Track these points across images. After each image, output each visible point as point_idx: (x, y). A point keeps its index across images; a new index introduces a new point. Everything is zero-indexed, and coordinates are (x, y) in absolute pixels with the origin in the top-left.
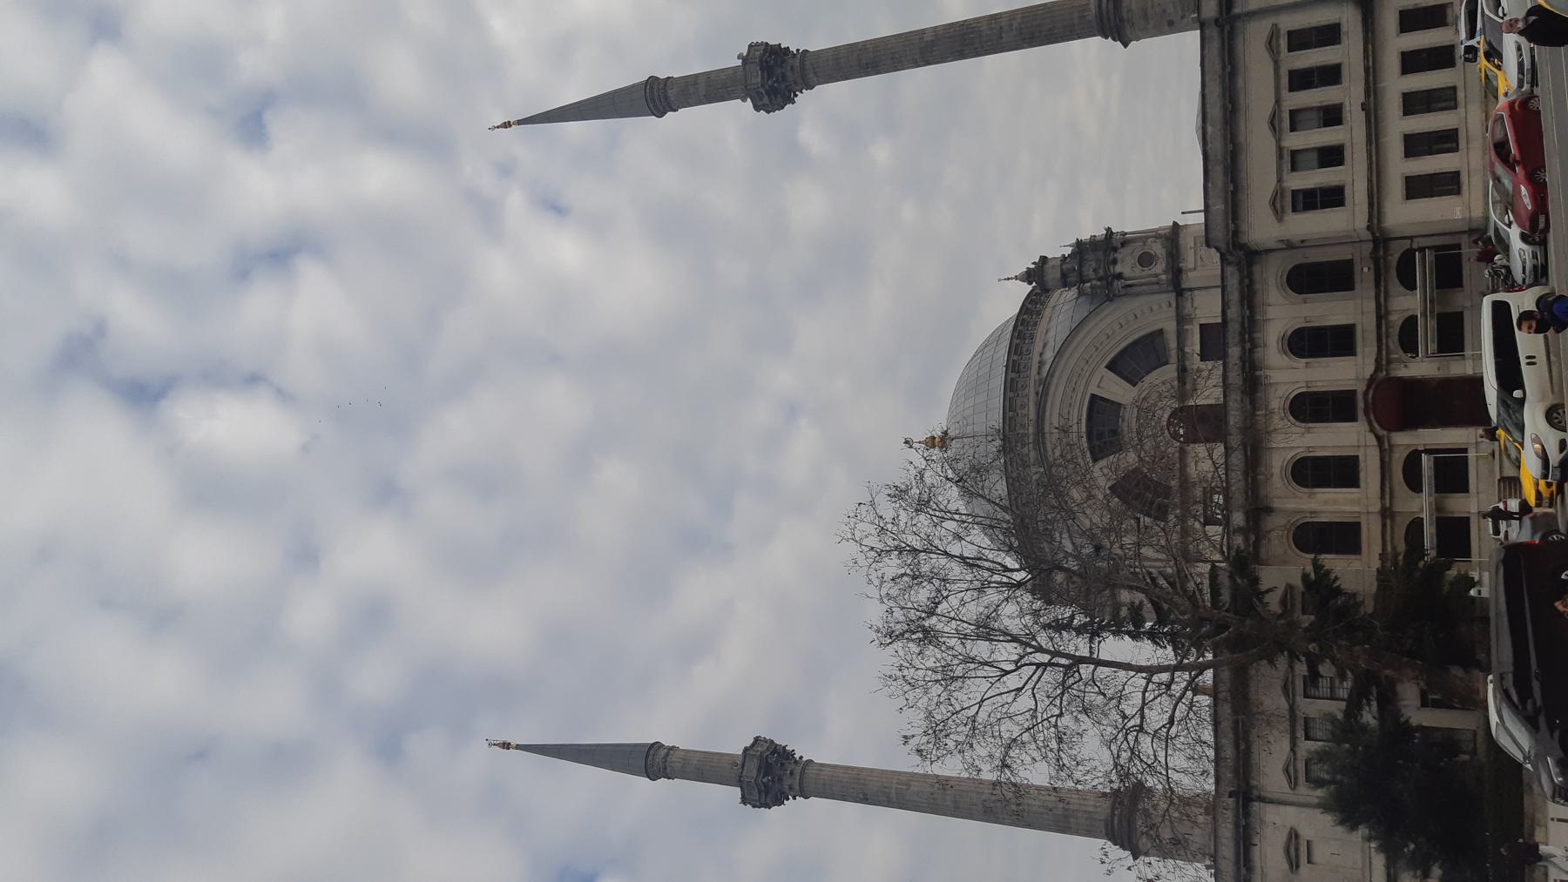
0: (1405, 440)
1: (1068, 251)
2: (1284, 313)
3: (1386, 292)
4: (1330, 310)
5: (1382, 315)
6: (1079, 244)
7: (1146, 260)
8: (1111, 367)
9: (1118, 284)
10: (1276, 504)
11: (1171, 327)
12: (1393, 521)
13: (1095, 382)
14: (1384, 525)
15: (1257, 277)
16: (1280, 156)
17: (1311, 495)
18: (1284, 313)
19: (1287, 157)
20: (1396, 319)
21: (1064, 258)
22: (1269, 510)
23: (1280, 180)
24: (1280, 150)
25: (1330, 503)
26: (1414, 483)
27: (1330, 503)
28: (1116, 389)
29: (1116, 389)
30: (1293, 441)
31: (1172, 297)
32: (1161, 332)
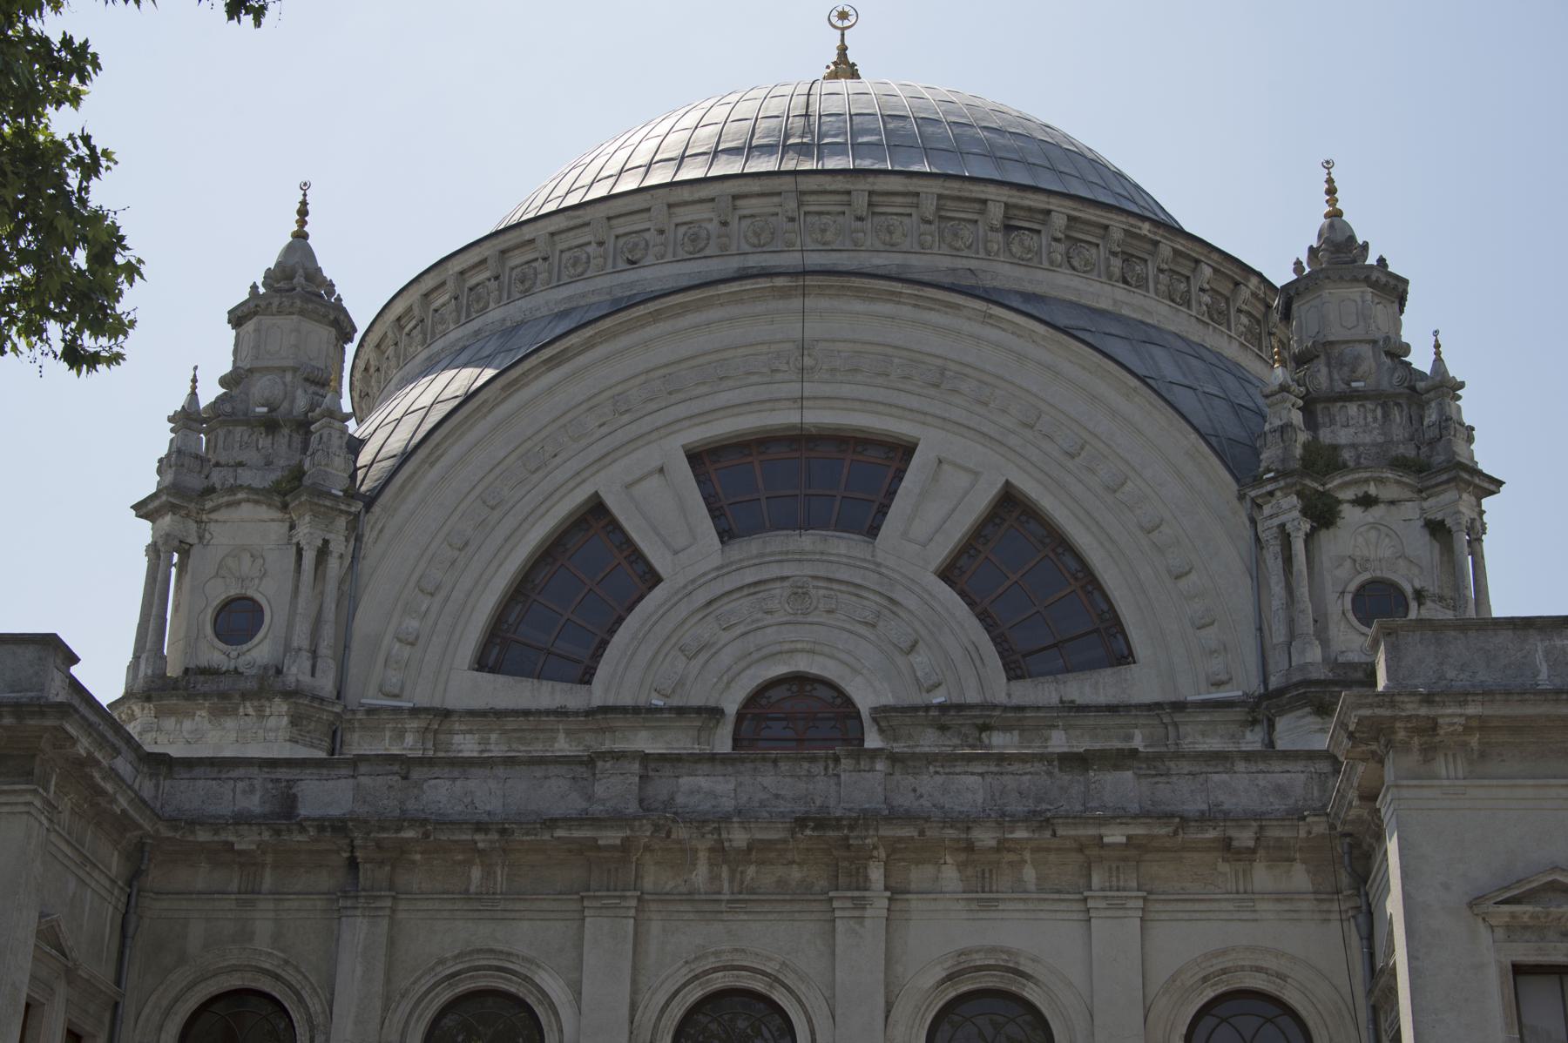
6: (1445, 387)
7: (1378, 601)
8: (1010, 502)
11: (1141, 683)
21: (1397, 352)
28: (933, 513)
29: (933, 513)
31: (1244, 684)
32: (1125, 657)
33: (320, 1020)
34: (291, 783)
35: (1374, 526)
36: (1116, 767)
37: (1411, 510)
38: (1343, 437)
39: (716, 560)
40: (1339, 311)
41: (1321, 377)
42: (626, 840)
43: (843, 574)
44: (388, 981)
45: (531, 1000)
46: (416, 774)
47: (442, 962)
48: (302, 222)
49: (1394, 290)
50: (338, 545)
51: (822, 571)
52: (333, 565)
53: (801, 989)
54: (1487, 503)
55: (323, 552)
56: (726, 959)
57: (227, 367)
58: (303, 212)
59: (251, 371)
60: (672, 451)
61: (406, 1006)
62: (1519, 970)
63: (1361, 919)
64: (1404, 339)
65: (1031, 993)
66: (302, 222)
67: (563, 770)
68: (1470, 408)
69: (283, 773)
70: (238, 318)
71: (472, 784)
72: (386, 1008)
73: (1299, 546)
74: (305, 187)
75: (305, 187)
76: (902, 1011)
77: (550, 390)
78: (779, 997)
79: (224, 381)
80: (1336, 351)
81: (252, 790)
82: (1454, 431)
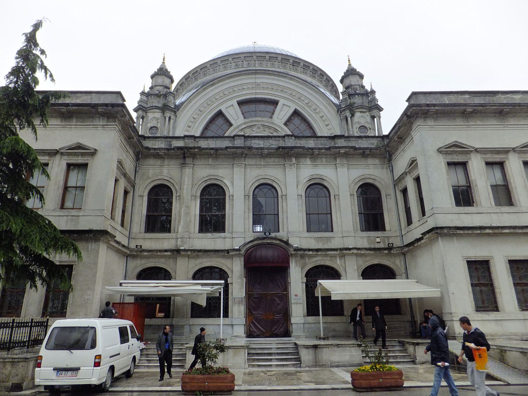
0: (236, 269)
1: (368, 88)
2: (343, 179)
3: (361, 255)
4: (346, 213)
5: (344, 252)
6: (373, 92)
8: (296, 113)
9: (348, 114)
10: (188, 171)
12: (169, 257)
13: (286, 102)
14: (166, 251)
15: (370, 161)
16: (498, 151)
17: (194, 197)
18: (343, 179)
19: (497, 158)
20: (337, 264)
21: (363, 87)
22: (183, 165)
23: (477, 150)
24: (506, 151)
25: (186, 211)
26: (200, 274)
27: (186, 211)
28: (282, 114)
29: (282, 114)
30: (238, 183)
33: (178, 190)
34: (170, 142)
35: (362, 116)
36: (341, 139)
37: (368, 114)
38: (355, 101)
39: (243, 122)
40: (353, 80)
41: (351, 91)
42: (242, 151)
43: (266, 124)
44: (192, 181)
45: (223, 186)
46: (197, 140)
47: (204, 178)
48: (164, 60)
49: (361, 77)
50: (172, 117)
51: (262, 123)
52: (172, 121)
53: (279, 182)
54: (381, 113)
55: (170, 118)
56: (263, 177)
57: (150, 85)
58: (164, 59)
59: (155, 86)
60: (234, 102)
61: (196, 187)
62: (449, 164)
63: (391, 168)
64: (364, 84)
65: (325, 184)
66: (164, 60)
67: (228, 139)
68: (377, 96)
69: (168, 140)
70: (152, 77)
71: (209, 142)
72: (192, 187)
73: (349, 119)
74: (164, 54)
75: (164, 54)
76: (300, 187)
77: (212, 90)
78: (274, 184)
79: (150, 88)
80: (352, 87)
81: (162, 143)
82: (375, 100)
